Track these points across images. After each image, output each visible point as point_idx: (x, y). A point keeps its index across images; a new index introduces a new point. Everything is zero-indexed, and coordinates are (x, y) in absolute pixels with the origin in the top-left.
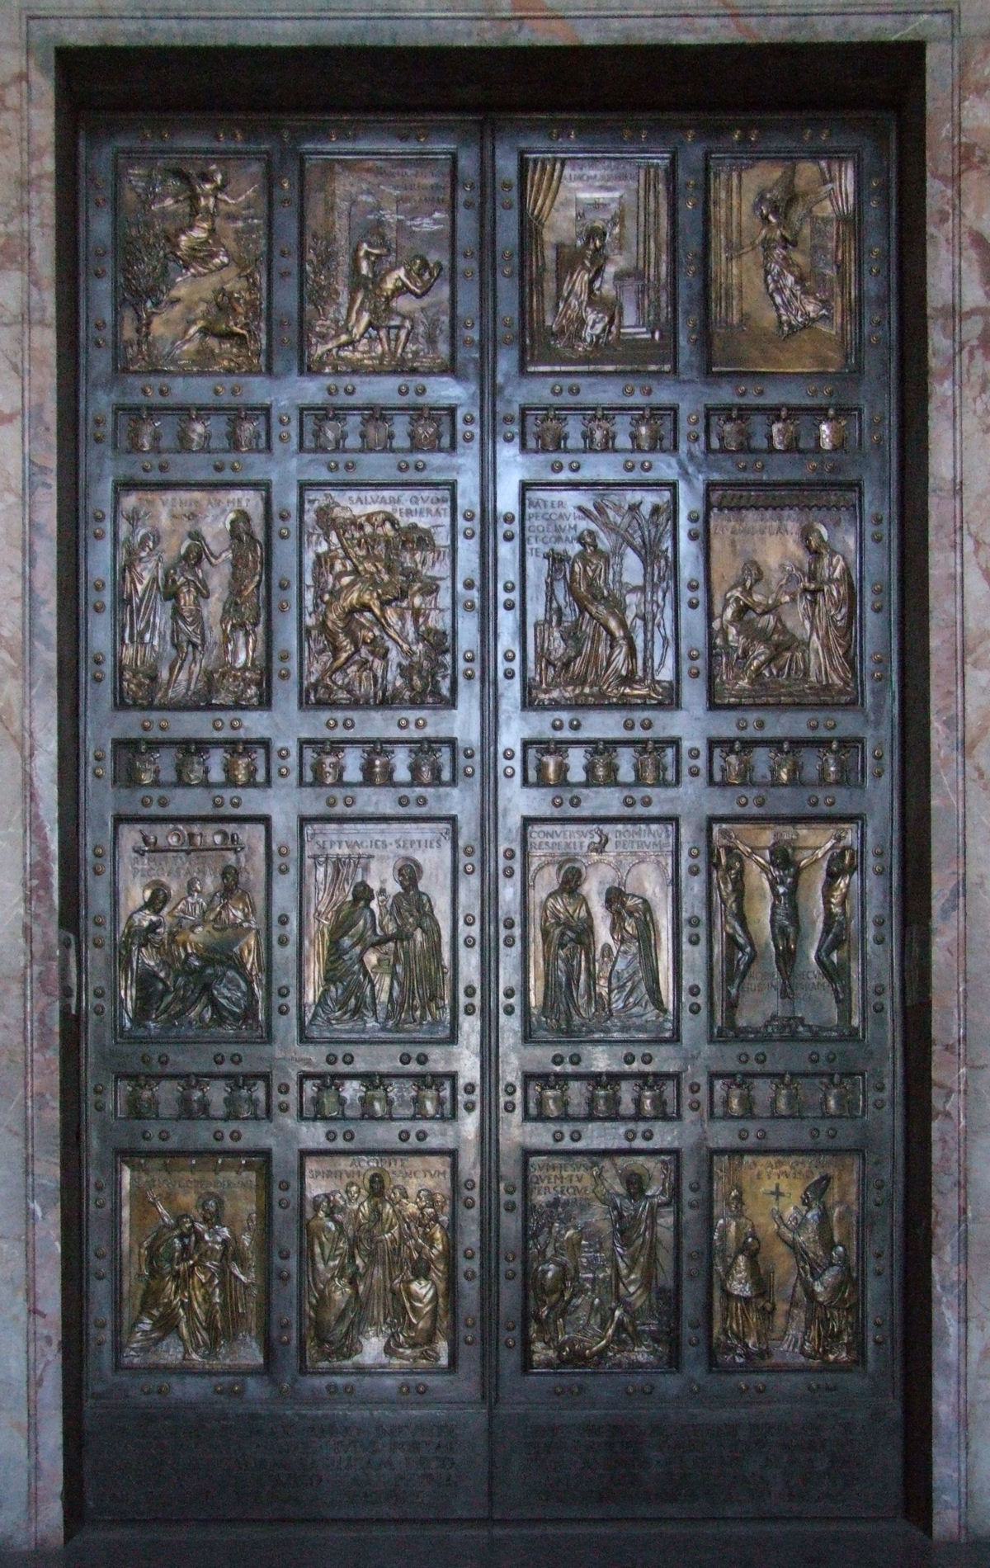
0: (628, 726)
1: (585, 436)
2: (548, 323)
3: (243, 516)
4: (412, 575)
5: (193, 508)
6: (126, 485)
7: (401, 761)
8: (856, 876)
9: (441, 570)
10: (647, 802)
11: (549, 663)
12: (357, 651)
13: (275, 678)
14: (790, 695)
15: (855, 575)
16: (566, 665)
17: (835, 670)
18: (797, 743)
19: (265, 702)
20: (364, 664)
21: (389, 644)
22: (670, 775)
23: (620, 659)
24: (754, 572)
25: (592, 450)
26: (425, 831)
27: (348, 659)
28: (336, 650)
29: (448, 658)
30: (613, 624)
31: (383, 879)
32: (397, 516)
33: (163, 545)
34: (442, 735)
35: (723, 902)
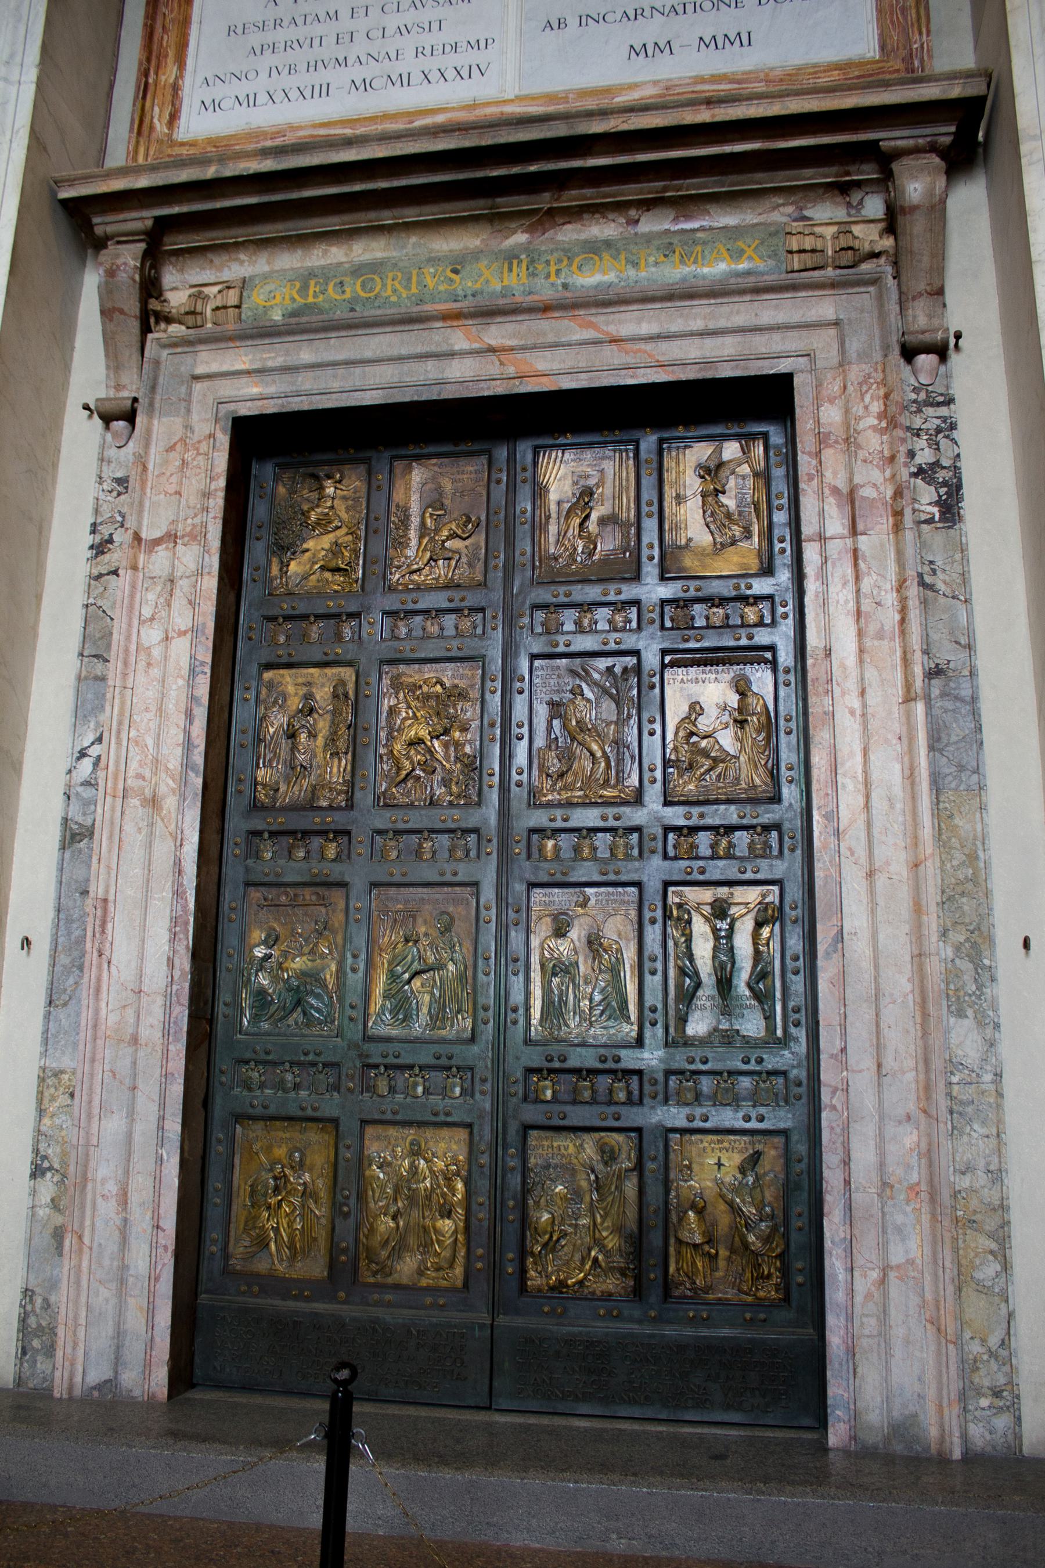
0: (604, 818)
1: (576, 623)
2: (552, 551)
3: (342, 683)
4: (453, 718)
5: (309, 679)
6: (269, 666)
8: (777, 925)
10: (617, 873)
11: (548, 775)
12: (413, 770)
13: (356, 788)
14: (725, 794)
15: (771, 707)
16: (562, 775)
17: (759, 776)
18: (731, 829)
20: (419, 778)
21: (436, 765)
22: (636, 852)
24: (696, 709)
25: (582, 632)
27: (407, 775)
28: (399, 769)
29: (477, 772)
30: (595, 747)
32: (445, 680)
33: (289, 703)
34: (471, 824)
35: (676, 944)
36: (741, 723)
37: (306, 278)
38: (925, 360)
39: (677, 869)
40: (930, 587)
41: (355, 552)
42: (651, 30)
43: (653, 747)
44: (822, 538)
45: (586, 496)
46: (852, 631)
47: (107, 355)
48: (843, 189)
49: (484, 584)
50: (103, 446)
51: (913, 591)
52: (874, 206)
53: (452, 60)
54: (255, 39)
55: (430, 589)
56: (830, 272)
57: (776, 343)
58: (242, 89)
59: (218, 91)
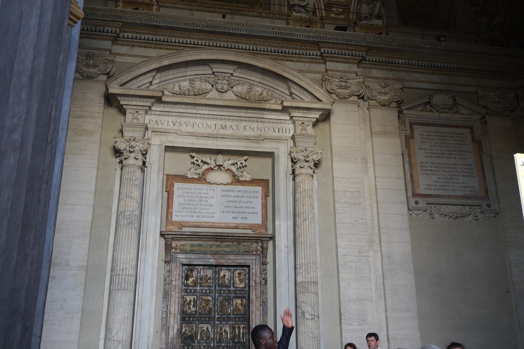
7: (207, 319)
9: (211, 303)
18: (240, 318)
19: (196, 314)
23: (226, 310)
24: (237, 303)
26: (209, 325)
31: (205, 329)
36: (242, 305)
37: (192, 246)
38: (264, 265)
39: (234, 323)
40: (263, 292)
41: (196, 281)
42: (235, 215)
43: (232, 308)
44: (252, 286)
45: (224, 275)
46: (255, 297)
47: (165, 254)
48: (257, 242)
49: (212, 287)
50: (165, 266)
51: (262, 293)
52: (260, 244)
53: (210, 215)
54: (183, 206)
55: (206, 287)
56: (255, 252)
57: (248, 261)
58: (181, 214)
59: (178, 214)
